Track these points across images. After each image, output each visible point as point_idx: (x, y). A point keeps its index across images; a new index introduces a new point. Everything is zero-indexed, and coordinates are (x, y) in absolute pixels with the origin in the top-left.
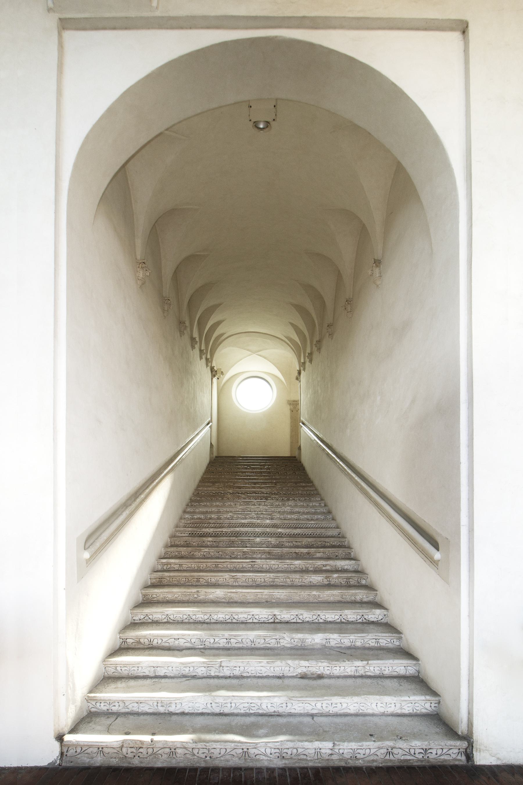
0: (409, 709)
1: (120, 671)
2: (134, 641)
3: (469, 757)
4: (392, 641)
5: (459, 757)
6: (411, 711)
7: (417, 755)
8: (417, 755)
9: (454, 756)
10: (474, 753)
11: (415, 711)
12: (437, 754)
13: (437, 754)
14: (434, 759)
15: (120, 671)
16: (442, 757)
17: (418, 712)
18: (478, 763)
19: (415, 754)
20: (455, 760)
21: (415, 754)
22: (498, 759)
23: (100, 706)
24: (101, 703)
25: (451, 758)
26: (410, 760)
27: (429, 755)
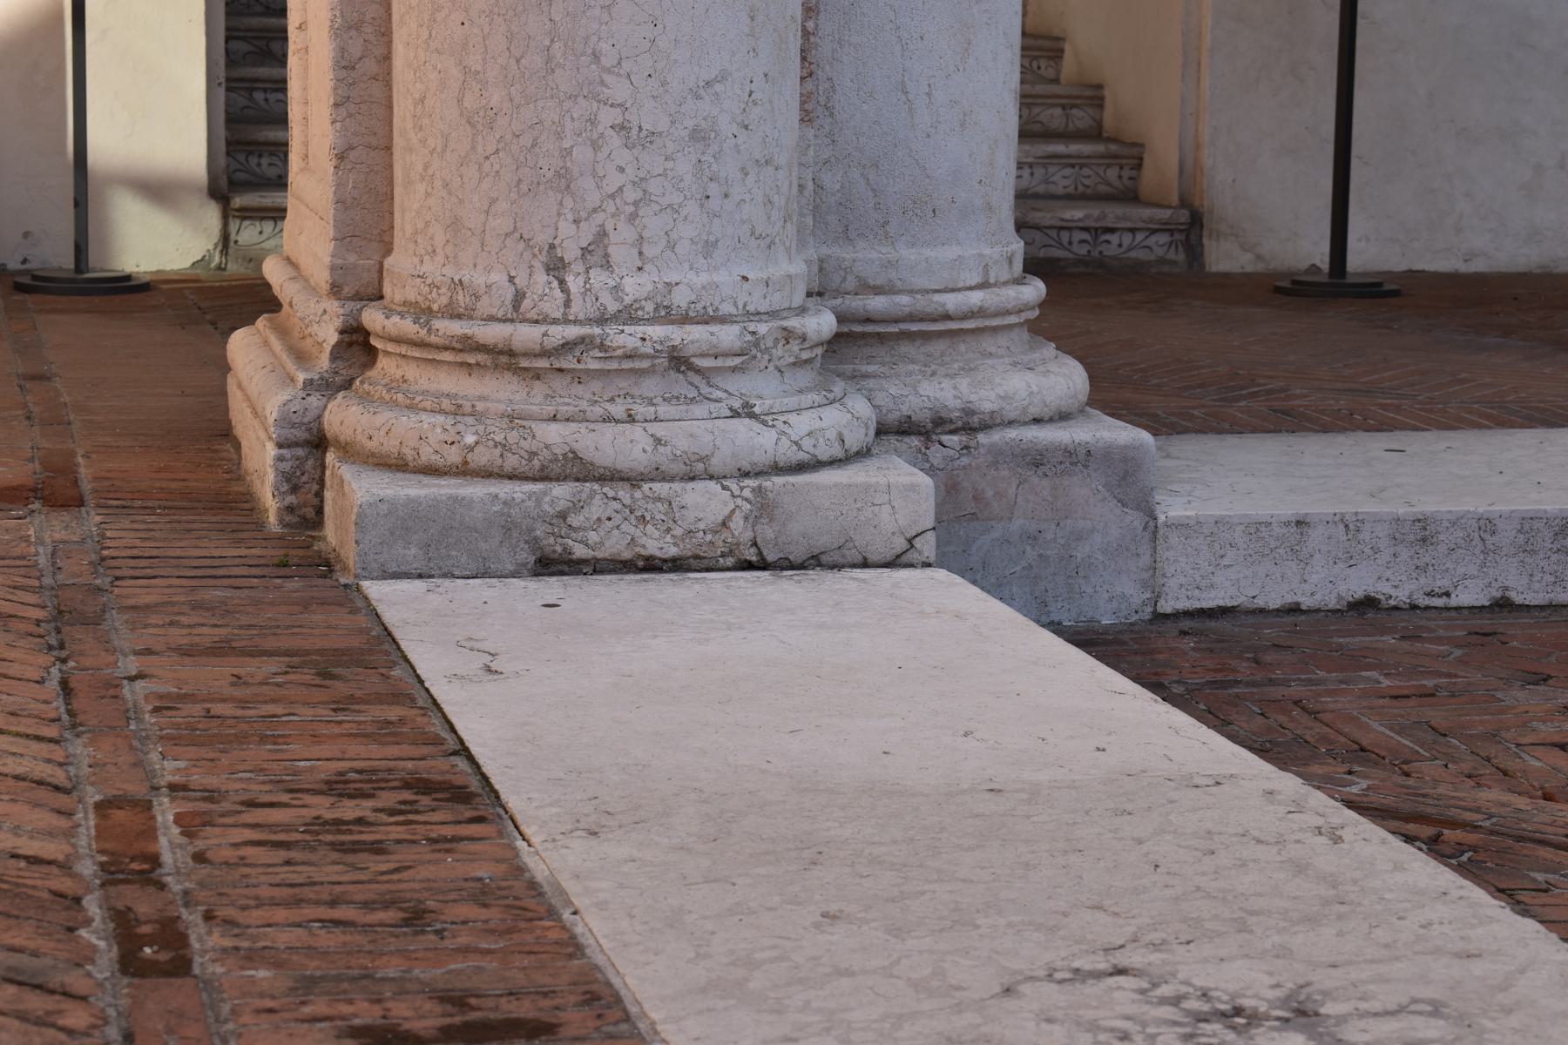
0: (1066, 182)
1: (262, 103)
2: (250, 48)
3: (1194, 252)
4: (1035, 65)
5: (1172, 255)
6: (1071, 190)
7: (1075, 248)
8: (1075, 248)
9: (1160, 252)
10: (1205, 241)
11: (1081, 188)
12: (1120, 245)
13: (1120, 245)
14: (1115, 258)
15: (262, 103)
16: (1132, 254)
17: (1089, 191)
18: (1214, 269)
19: (1070, 243)
20: (1162, 261)
21: (1070, 243)
22: (1259, 257)
23: (259, 165)
24: (260, 156)
25: (1153, 257)
26: (1059, 259)
27: (1103, 247)
